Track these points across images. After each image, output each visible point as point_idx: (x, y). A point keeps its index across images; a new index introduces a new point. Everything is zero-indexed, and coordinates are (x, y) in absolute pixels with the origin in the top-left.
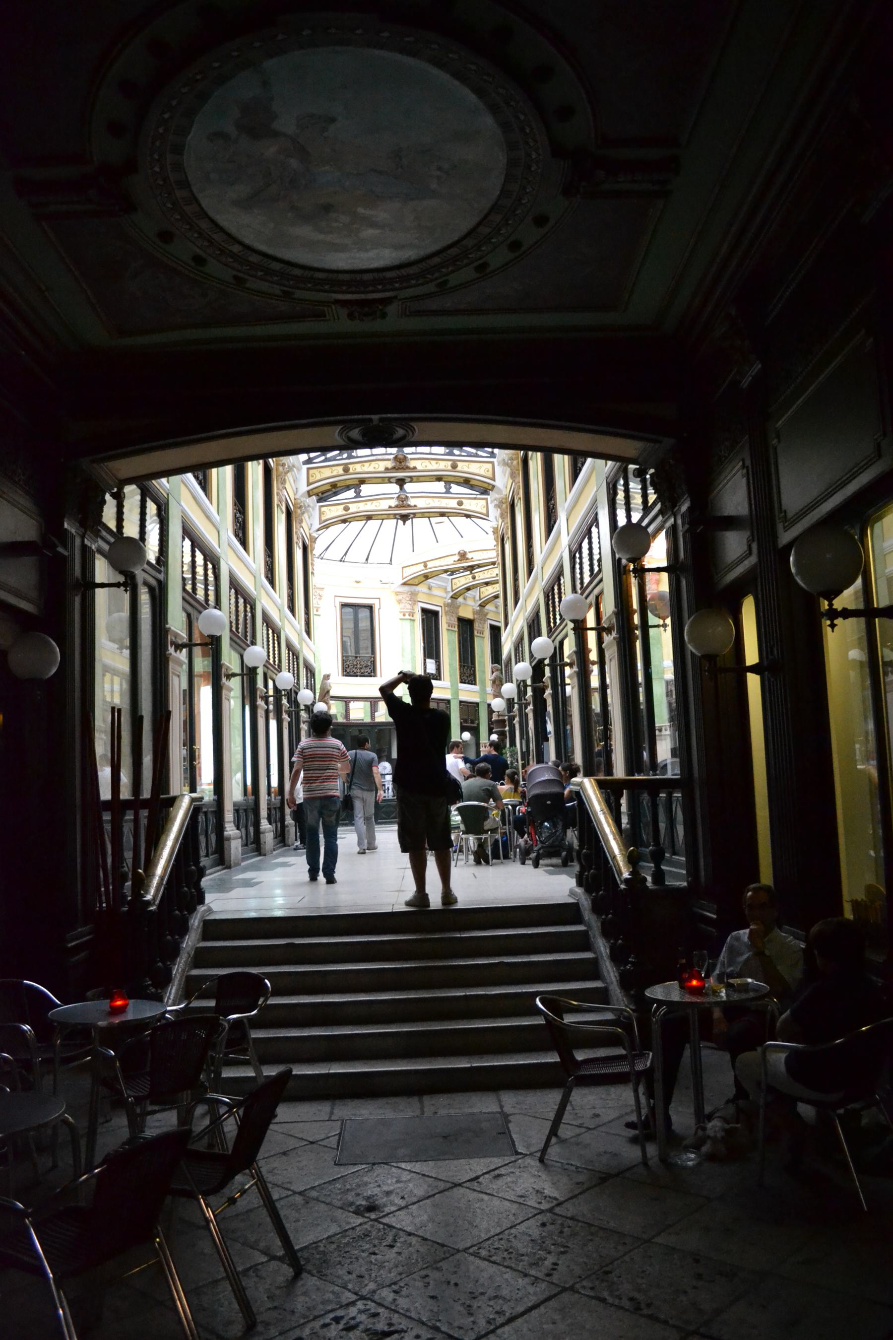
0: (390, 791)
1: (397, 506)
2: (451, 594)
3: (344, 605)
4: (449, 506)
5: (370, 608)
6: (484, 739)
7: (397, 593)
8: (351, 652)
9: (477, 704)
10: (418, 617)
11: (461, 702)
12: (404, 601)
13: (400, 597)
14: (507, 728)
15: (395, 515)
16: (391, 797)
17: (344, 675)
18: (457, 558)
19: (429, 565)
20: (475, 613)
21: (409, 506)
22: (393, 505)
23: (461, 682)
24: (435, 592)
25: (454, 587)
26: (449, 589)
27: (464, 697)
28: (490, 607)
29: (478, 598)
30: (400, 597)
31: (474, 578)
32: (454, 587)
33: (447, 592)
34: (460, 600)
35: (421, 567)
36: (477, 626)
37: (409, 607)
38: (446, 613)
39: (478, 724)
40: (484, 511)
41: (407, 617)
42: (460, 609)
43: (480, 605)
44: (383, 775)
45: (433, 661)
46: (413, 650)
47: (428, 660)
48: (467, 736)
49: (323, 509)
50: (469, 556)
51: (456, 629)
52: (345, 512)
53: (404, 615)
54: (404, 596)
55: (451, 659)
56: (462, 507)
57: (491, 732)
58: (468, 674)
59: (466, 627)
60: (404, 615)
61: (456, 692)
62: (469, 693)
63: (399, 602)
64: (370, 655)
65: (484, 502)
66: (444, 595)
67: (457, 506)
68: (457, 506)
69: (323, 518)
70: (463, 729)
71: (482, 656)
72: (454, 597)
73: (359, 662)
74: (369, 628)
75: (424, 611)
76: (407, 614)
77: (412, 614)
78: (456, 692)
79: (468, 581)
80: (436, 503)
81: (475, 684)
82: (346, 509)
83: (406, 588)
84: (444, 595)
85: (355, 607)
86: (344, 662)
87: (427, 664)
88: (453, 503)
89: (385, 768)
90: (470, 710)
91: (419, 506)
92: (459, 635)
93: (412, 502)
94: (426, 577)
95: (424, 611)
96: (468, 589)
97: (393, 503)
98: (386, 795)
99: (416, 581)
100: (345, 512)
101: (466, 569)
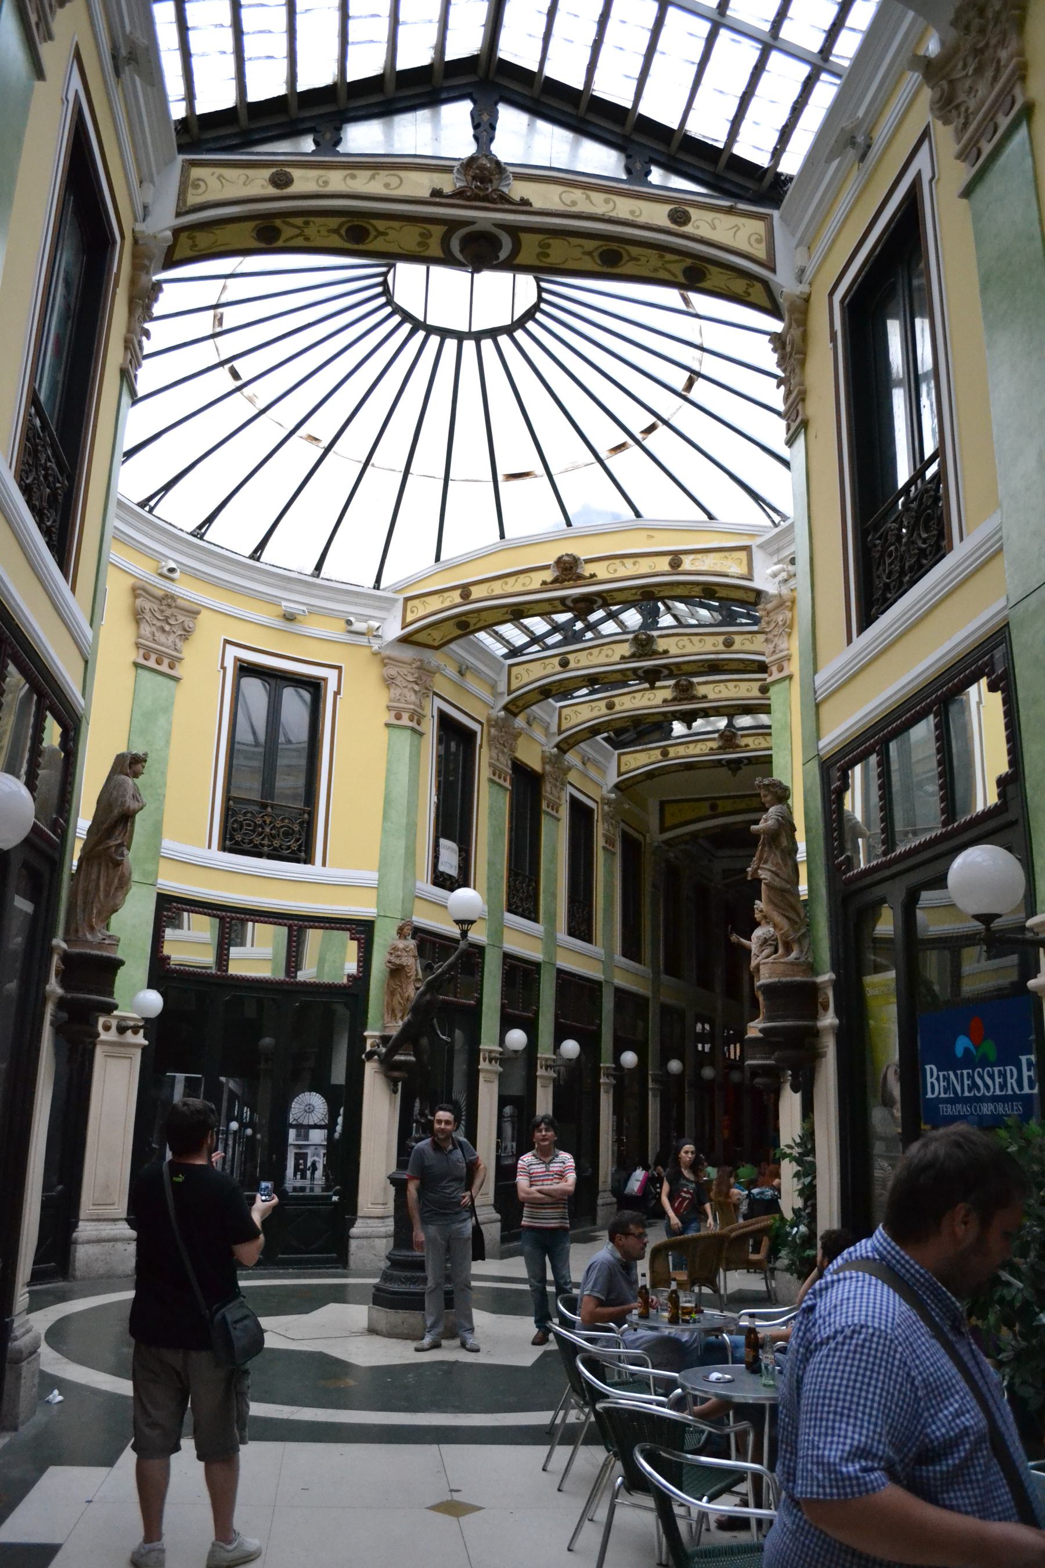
0: (319, 1173)
1: (459, 194)
2: (507, 699)
3: (245, 669)
4: (642, 220)
5: (314, 687)
6: (545, 1052)
7: (385, 661)
8: (251, 788)
9: (537, 965)
10: (430, 728)
11: (507, 956)
12: (399, 681)
13: (393, 672)
14: (829, 1020)
15: (453, 225)
16: (318, 1191)
17: (223, 848)
18: (548, 576)
19: (477, 592)
20: (545, 760)
21: (505, 199)
22: (448, 189)
23: (510, 911)
24: (472, 683)
25: (515, 684)
26: (502, 687)
27: (515, 945)
28: (572, 758)
29: (554, 728)
30: (393, 672)
31: (564, 664)
32: (515, 684)
33: (496, 694)
34: (520, 722)
35: (456, 597)
36: (547, 788)
37: (412, 697)
38: (492, 740)
39: (537, 1013)
40: (761, 253)
41: (405, 721)
42: (521, 741)
43: (557, 746)
44: (303, 1130)
45: (454, 846)
46: (412, 807)
47: (443, 842)
48: (517, 1038)
49: (196, 172)
50: (587, 570)
51: (507, 784)
52: (272, 191)
53: (398, 717)
54: (404, 671)
55: (493, 849)
56: (688, 229)
57: (559, 1038)
58: (522, 895)
59: (527, 787)
60: (398, 717)
61: (497, 931)
62: (523, 938)
63: (389, 682)
64: (300, 805)
65: (759, 226)
66: (490, 699)
67: (665, 222)
68: (665, 222)
69: (194, 198)
70: (507, 1023)
71: (553, 860)
72: (513, 709)
73: (271, 815)
74: (302, 791)
75: (445, 720)
76: (405, 716)
77: (417, 716)
78: (497, 931)
79: (549, 671)
80: (598, 204)
81: (536, 920)
82: (281, 180)
83: (408, 653)
84: (490, 699)
85: (275, 679)
86: (228, 812)
87: (442, 851)
88: (658, 215)
89: (310, 1109)
90: (520, 974)
91: (538, 204)
92: (511, 798)
93: (518, 190)
94: (465, 625)
95: (445, 720)
96: (546, 692)
97: (448, 183)
98: (307, 1183)
99: (437, 636)
100: (272, 191)
101: (564, 604)
